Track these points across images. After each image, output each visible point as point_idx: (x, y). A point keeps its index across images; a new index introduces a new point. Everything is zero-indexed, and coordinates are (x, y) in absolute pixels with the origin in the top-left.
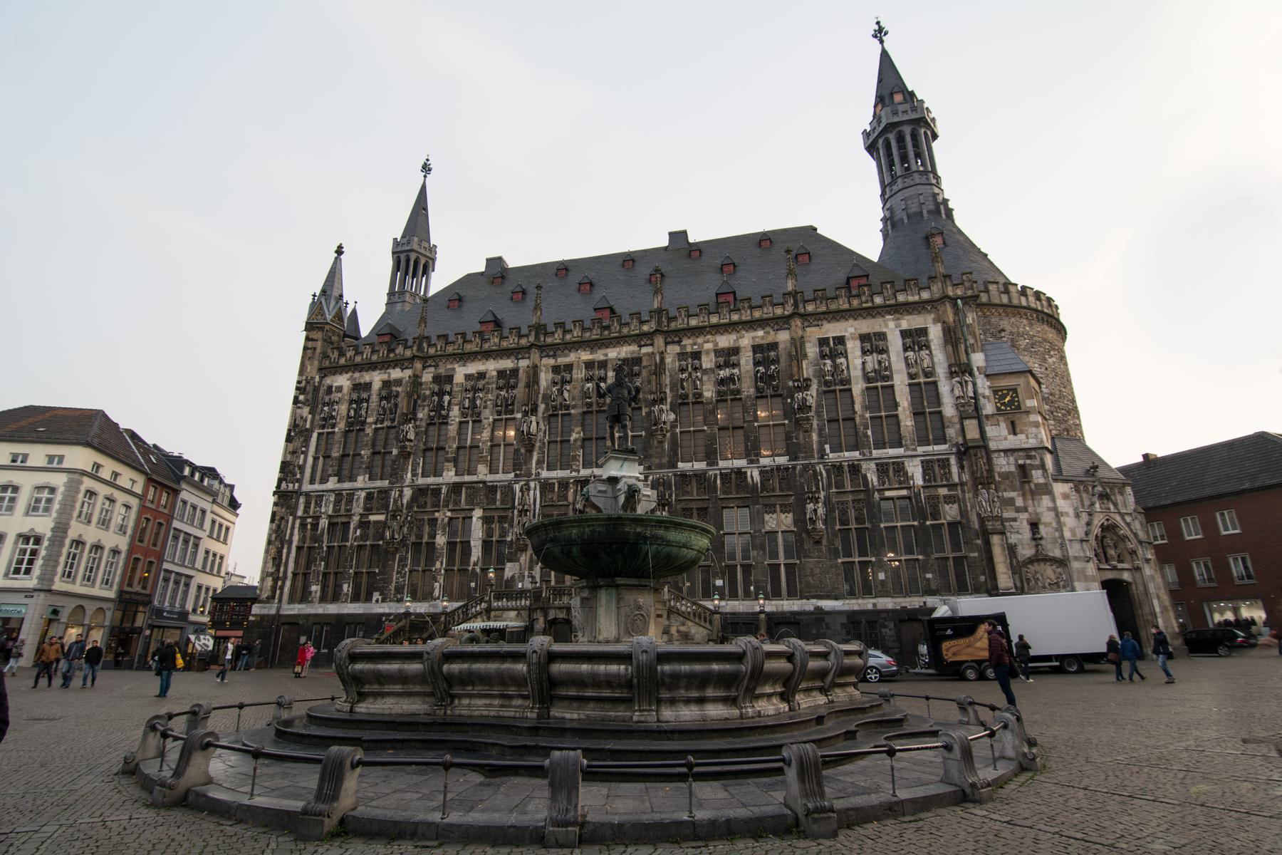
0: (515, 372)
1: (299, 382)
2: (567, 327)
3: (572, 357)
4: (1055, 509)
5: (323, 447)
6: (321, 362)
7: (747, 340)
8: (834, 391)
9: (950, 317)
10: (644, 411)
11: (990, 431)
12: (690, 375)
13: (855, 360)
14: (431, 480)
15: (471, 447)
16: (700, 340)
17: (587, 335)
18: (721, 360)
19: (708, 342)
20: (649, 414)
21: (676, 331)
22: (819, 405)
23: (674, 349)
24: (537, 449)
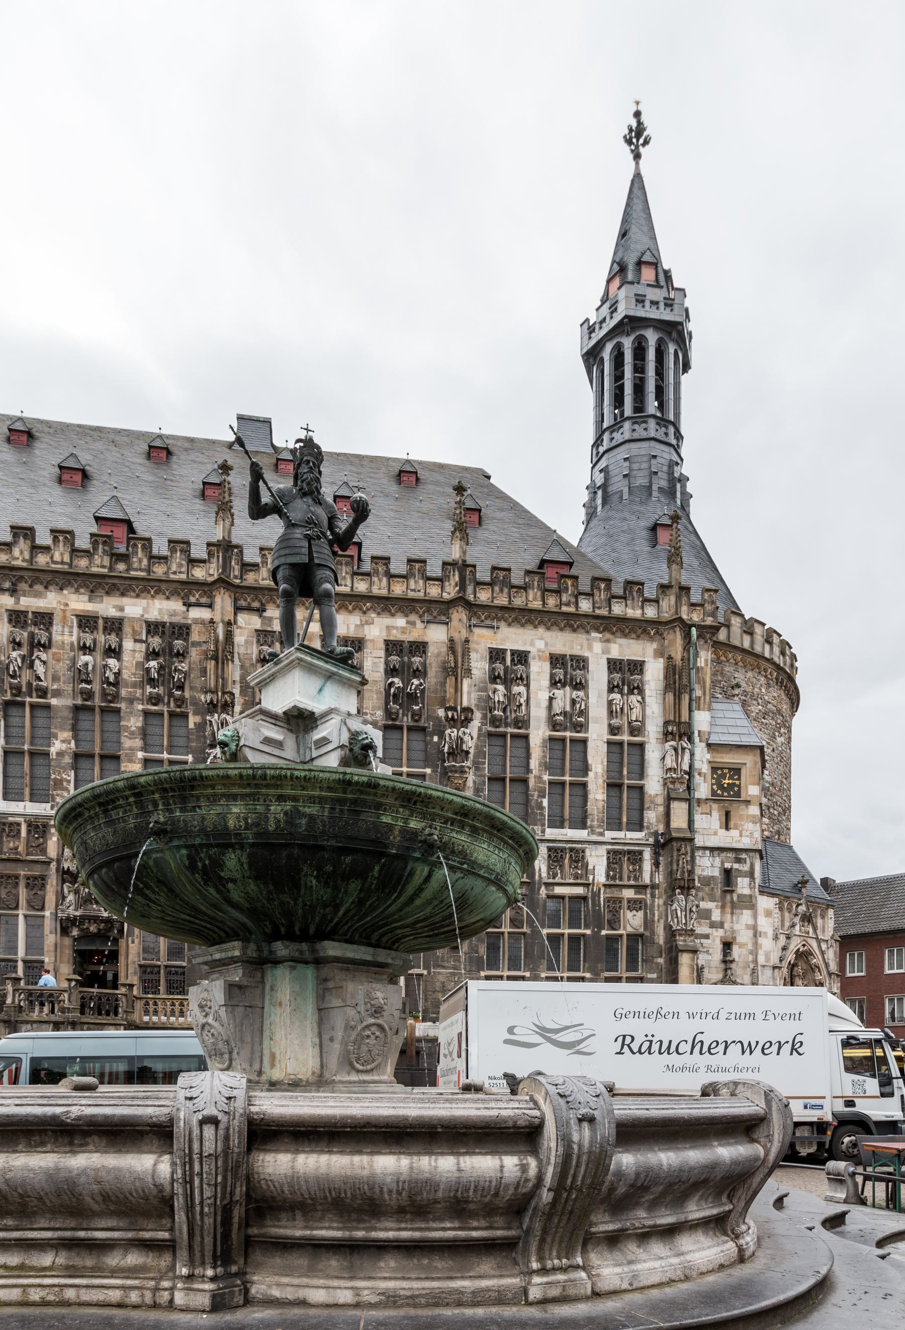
4: (754, 928)
7: (378, 629)
8: (504, 735)
9: (677, 652)
11: (700, 821)
13: (540, 695)
22: (480, 753)
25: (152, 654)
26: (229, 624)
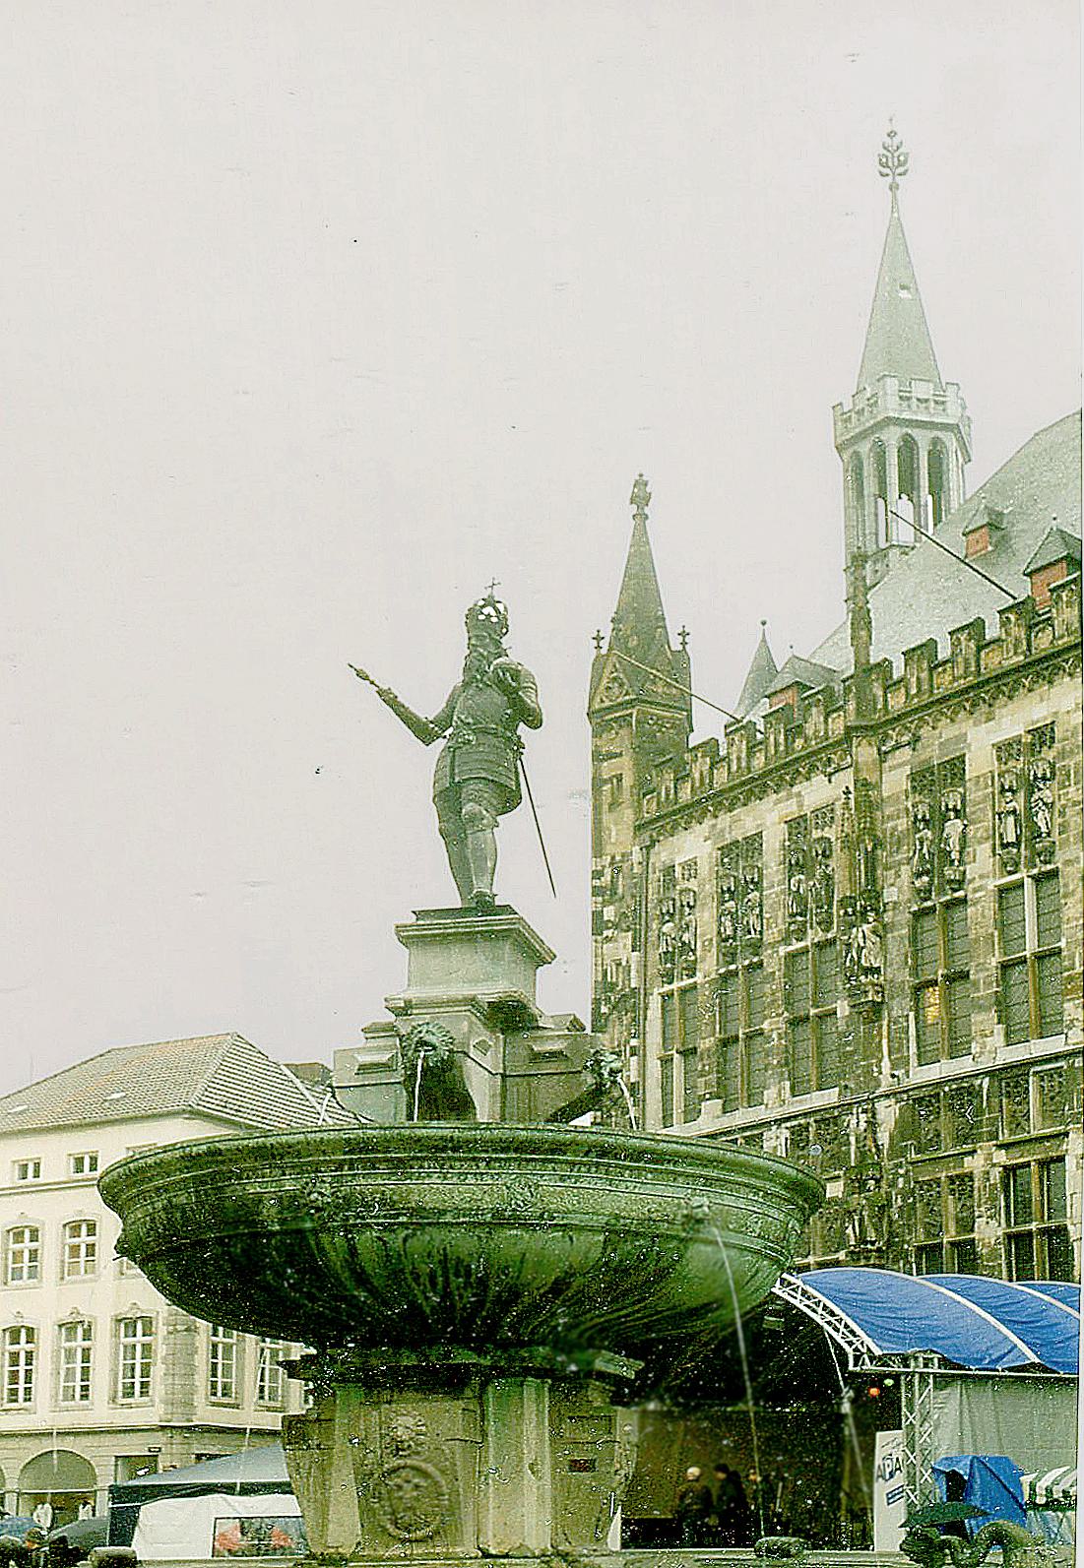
1: (597, 874)
5: (676, 1030)
6: (638, 809)
14: (945, 1069)
15: (1040, 958)
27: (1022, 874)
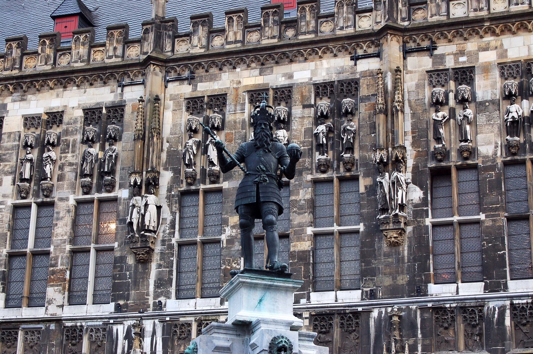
0: (117, 110)
2: (216, 26)
3: (225, 81)
10: (363, 183)
12: (452, 112)
15: (35, 254)
16: (471, 45)
17: (253, 37)
18: (513, 84)
19: (486, 49)
20: (372, 189)
21: (427, 29)
23: (421, 63)
24: (156, 258)
25: (320, 118)
26: (398, 70)
27: (30, 200)
